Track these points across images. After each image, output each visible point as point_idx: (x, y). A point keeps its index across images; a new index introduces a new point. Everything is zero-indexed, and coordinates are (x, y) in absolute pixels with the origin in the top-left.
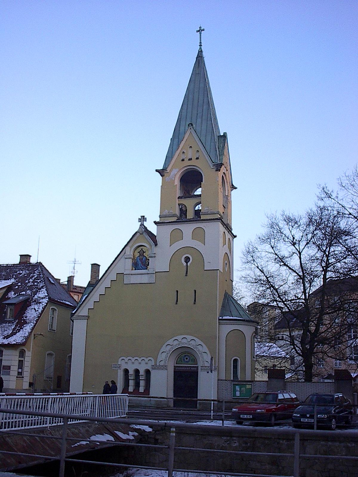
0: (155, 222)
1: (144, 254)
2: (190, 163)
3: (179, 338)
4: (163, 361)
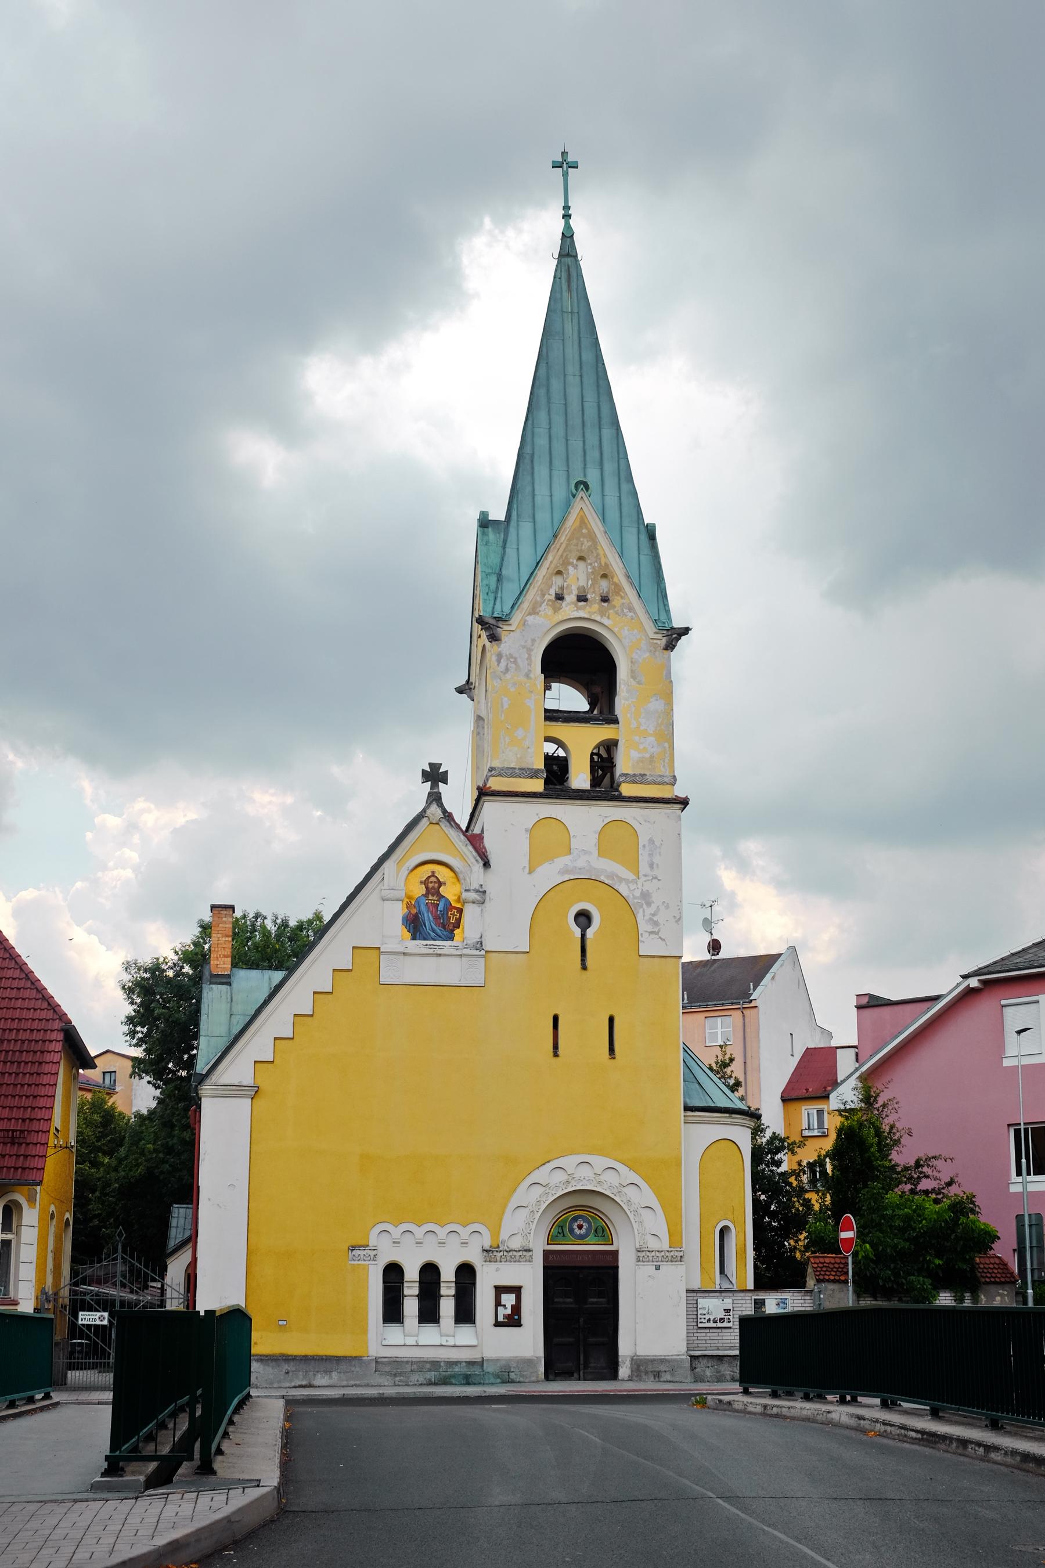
1: (441, 889)
2: (583, 611)
3: (569, 1162)
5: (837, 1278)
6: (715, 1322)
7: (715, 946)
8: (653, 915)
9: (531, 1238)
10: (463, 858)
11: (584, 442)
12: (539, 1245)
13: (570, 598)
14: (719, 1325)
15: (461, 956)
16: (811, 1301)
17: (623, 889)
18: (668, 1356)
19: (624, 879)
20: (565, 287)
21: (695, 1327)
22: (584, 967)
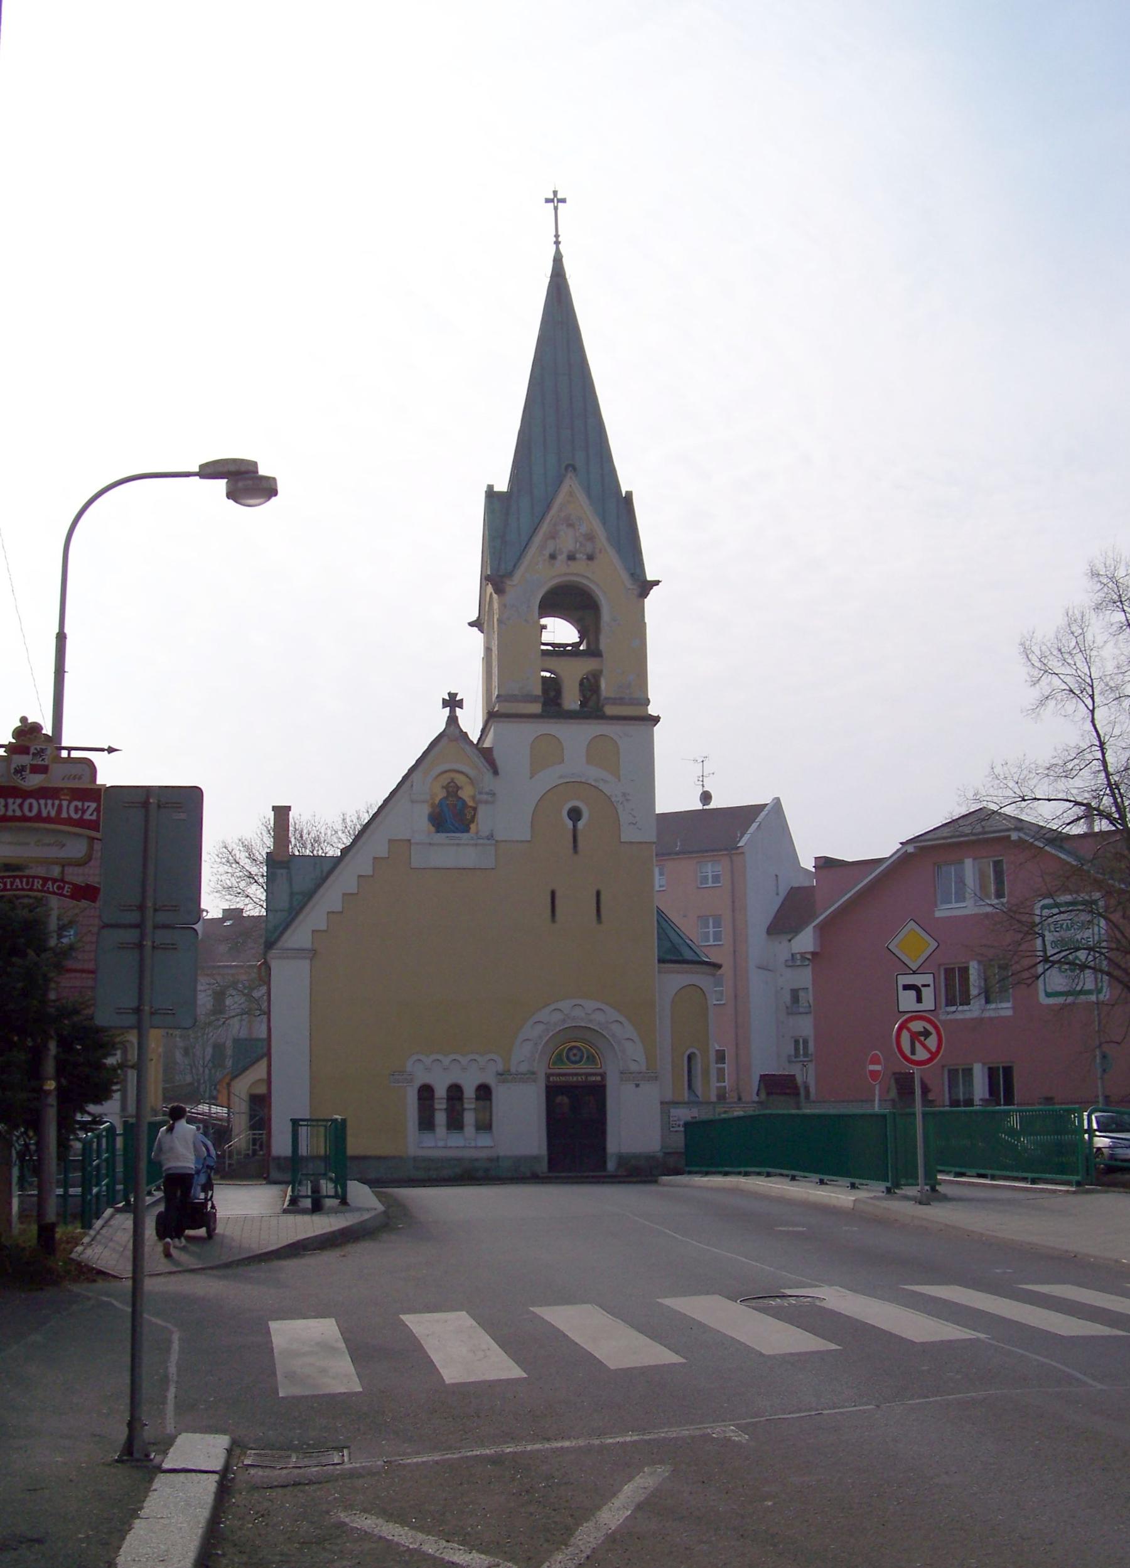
1: (459, 792)
3: (565, 1005)
12: (541, 1070)
13: (562, 558)
15: (476, 845)
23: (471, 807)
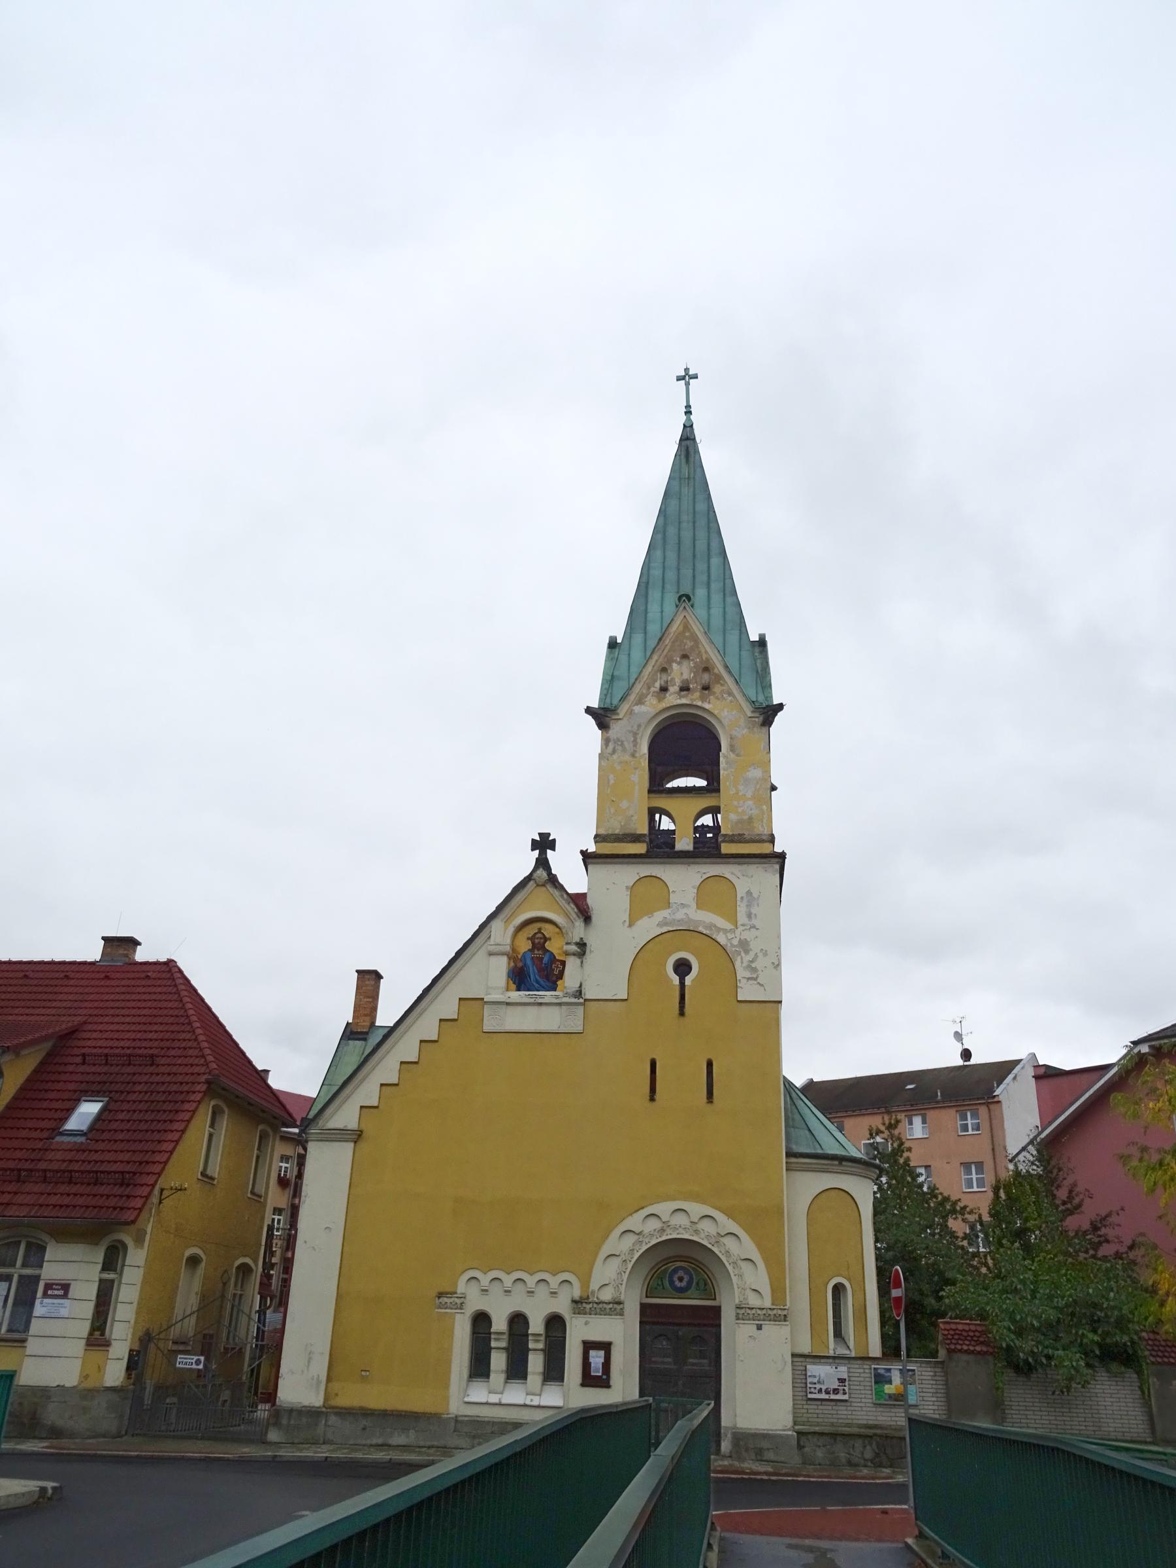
0: (583, 853)
3: (664, 1208)
4: (611, 1285)
5: (972, 1348)
6: (827, 1392)
7: (966, 1054)
8: (752, 962)
9: (623, 1288)
10: (567, 916)
11: (694, 570)
13: (673, 689)
14: (833, 1397)
15: (560, 1004)
16: (942, 1374)
17: (721, 939)
18: (772, 1430)
19: (723, 929)
20: (684, 460)
21: (804, 1398)
22: (682, 1013)
23: (558, 960)
